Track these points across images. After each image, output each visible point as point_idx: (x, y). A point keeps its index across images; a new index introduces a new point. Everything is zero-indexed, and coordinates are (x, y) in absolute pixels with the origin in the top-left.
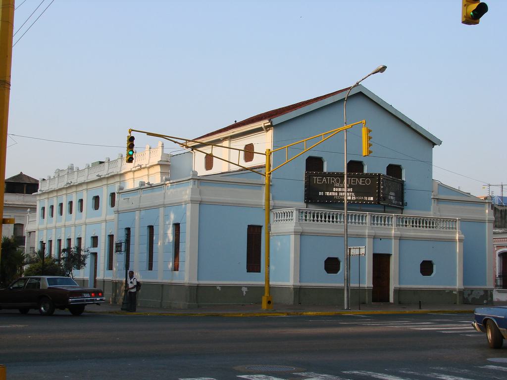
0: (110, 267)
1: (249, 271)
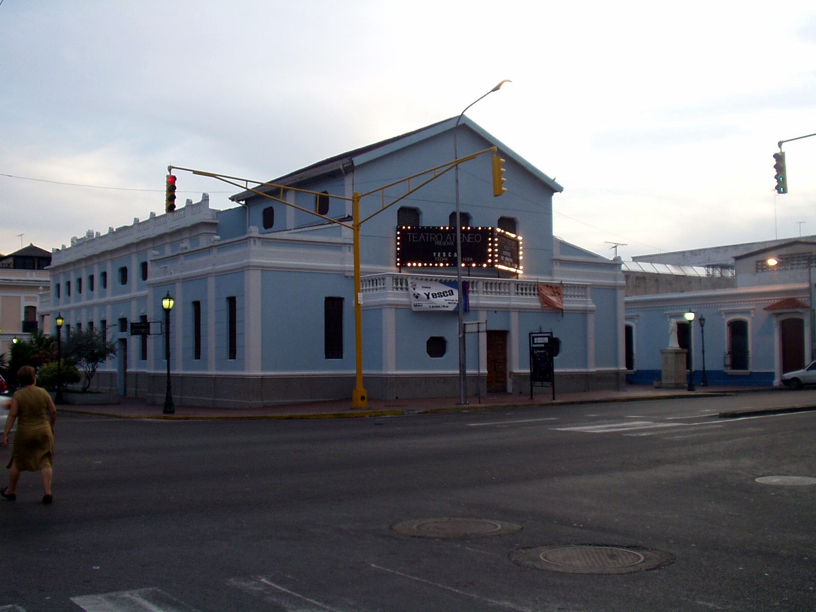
0: (144, 356)
1: (327, 357)
